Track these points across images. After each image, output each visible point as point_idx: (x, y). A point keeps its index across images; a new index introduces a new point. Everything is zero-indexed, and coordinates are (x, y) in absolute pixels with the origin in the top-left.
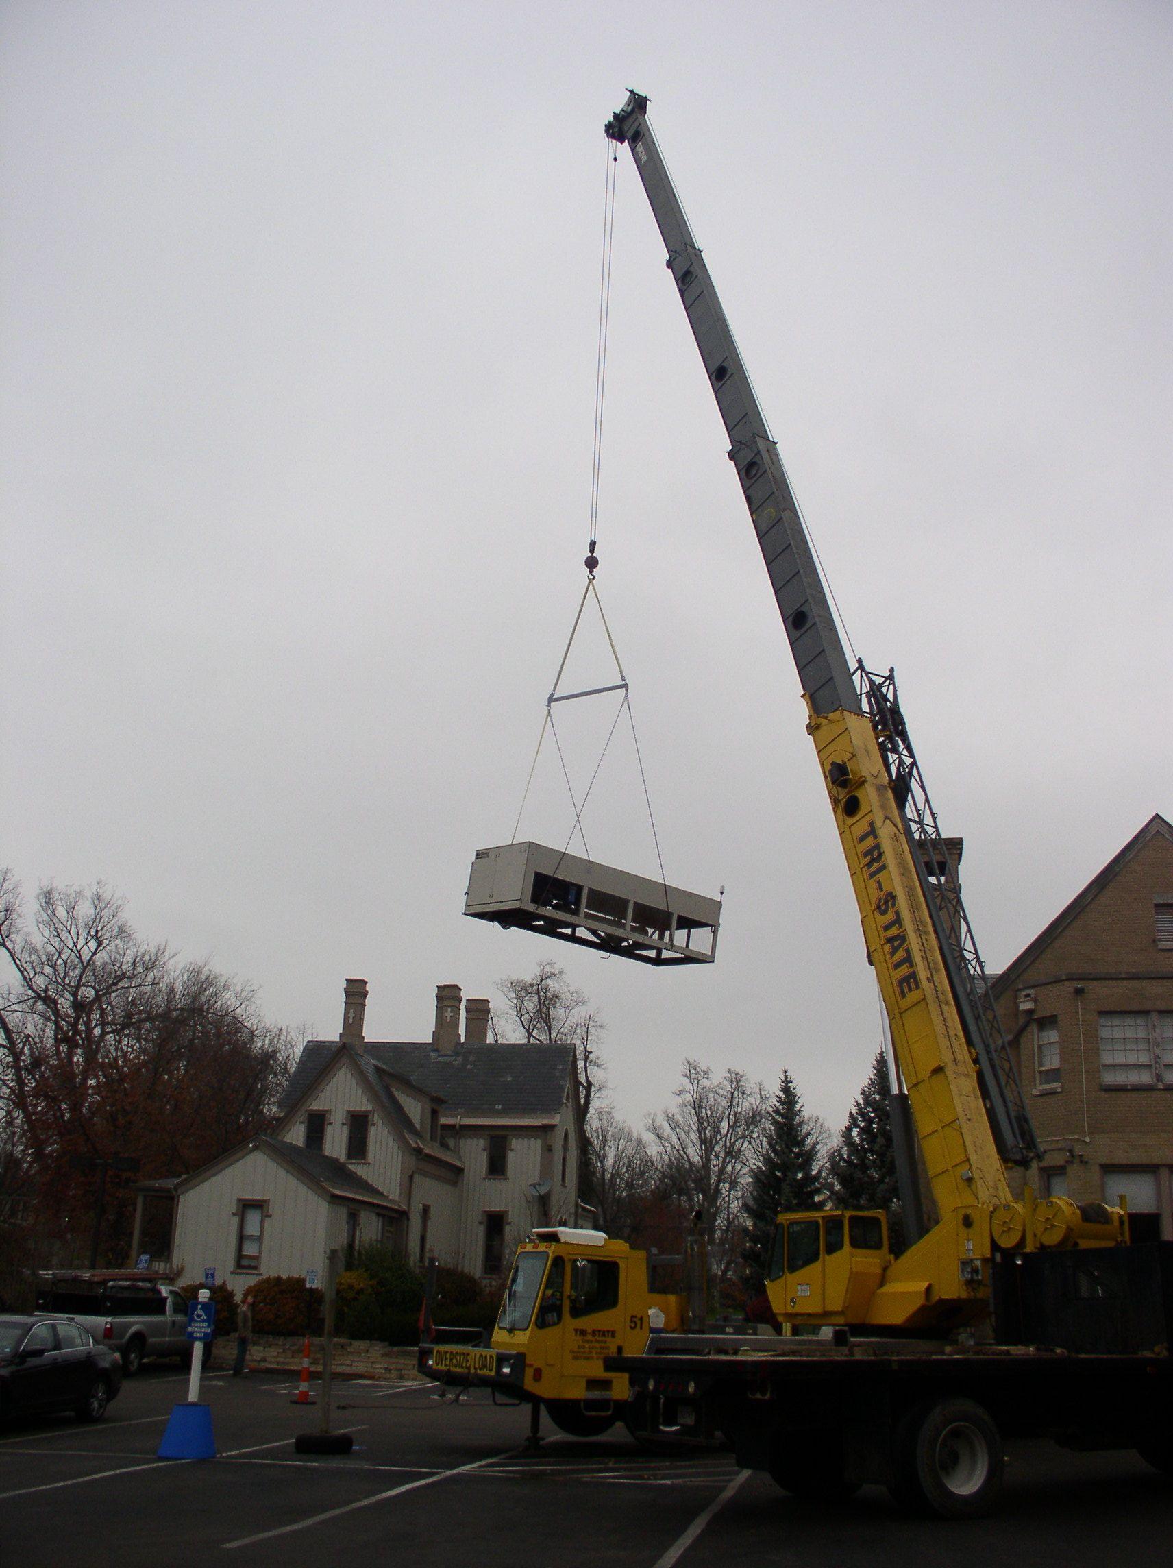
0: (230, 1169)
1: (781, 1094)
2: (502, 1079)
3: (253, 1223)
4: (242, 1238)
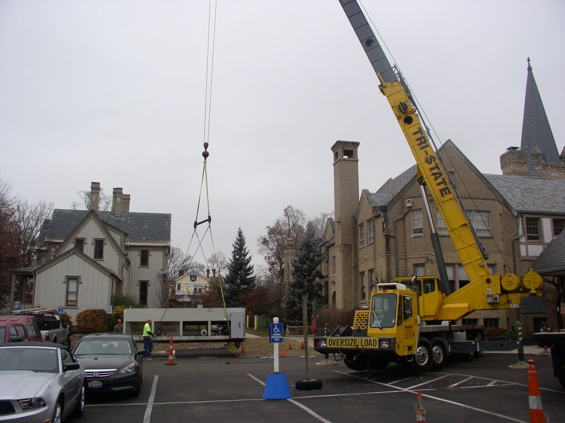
0: (61, 263)
1: (238, 237)
2: (143, 227)
3: (73, 286)
4: (68, 293)
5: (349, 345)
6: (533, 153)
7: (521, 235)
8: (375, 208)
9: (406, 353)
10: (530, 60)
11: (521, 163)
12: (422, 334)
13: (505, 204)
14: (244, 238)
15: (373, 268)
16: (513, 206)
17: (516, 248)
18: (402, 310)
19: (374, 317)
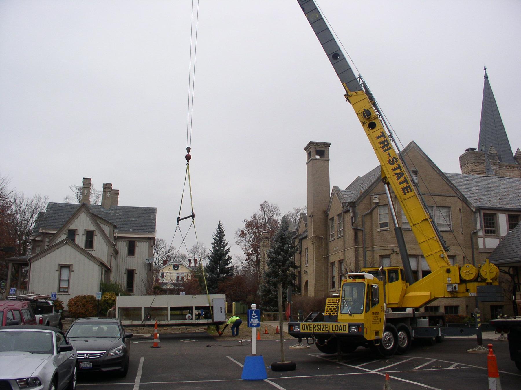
1: (218, 230)
2: (130, 220)
3: (65, 274)
4: (60, 280)
5: (321, 330)
6: (489, 153)
7: (479, 229)
8: (344, 204)
9: (373, 337)
10: (486, 69)
11: (479, 163)
12: (388, 320)
13: (464, 200)
14: (223, 231)
15: (343, 259)
16: (472, 202)
17: (474, 241)
18: (369, 298)
19: (344, 304)
